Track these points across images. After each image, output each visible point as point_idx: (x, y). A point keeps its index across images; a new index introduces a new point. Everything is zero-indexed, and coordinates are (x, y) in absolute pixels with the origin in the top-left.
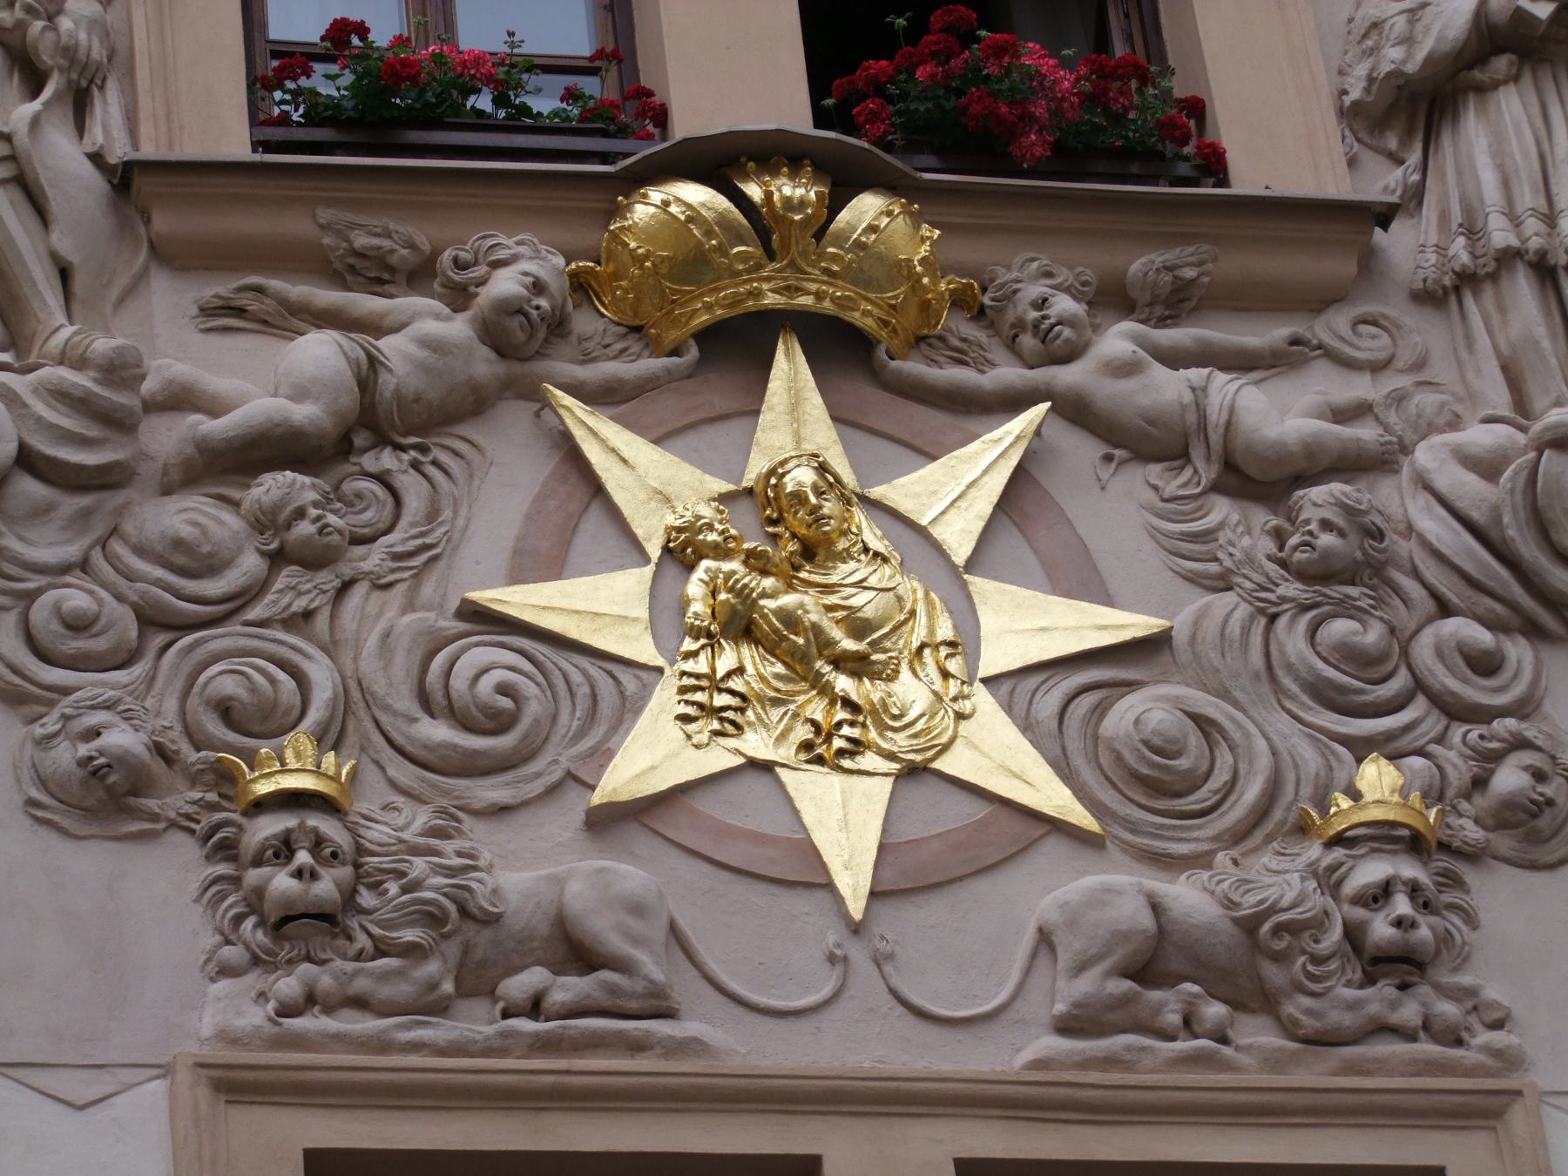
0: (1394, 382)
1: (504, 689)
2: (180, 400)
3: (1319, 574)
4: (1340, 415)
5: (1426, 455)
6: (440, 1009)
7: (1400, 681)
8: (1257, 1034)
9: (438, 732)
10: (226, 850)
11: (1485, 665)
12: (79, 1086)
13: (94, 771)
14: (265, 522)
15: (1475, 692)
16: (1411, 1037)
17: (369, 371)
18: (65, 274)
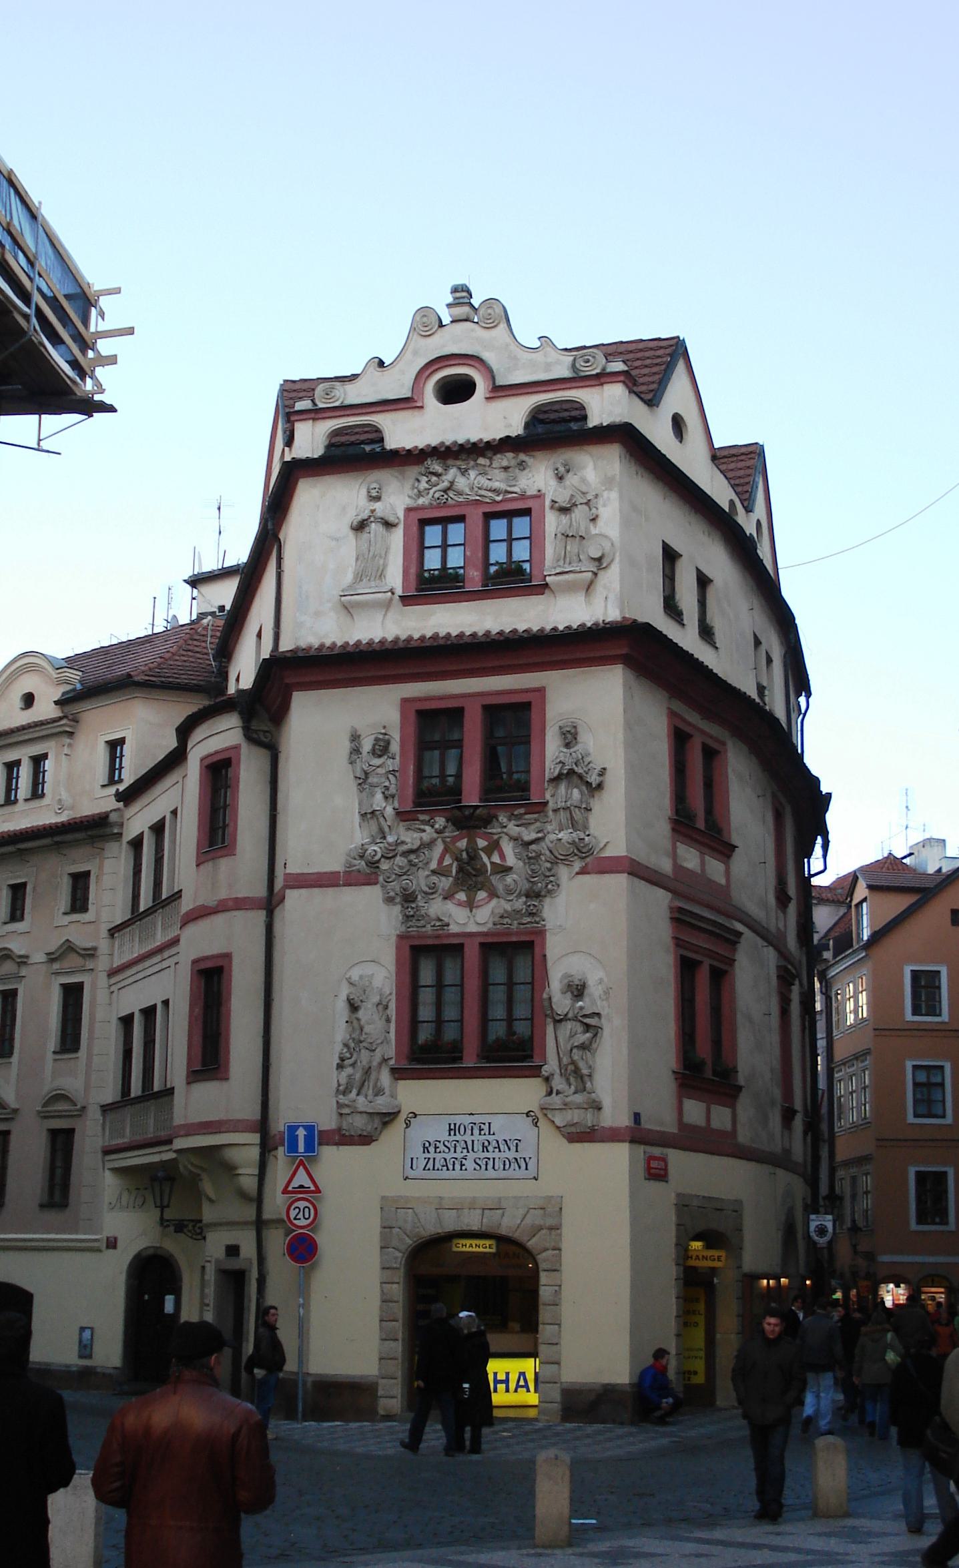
1: (434, 883)
2: (403, 842)
3: (530, 858)
5: (547, 840)
6: (424, 926)
7: (540, 872)
9: (426, 889)
10: (403, 907)
11: (550, 870)
14: (410, 861)
15: (548, 874)
16: (532, 923)
17: (421, 839)
18: (389, 826)
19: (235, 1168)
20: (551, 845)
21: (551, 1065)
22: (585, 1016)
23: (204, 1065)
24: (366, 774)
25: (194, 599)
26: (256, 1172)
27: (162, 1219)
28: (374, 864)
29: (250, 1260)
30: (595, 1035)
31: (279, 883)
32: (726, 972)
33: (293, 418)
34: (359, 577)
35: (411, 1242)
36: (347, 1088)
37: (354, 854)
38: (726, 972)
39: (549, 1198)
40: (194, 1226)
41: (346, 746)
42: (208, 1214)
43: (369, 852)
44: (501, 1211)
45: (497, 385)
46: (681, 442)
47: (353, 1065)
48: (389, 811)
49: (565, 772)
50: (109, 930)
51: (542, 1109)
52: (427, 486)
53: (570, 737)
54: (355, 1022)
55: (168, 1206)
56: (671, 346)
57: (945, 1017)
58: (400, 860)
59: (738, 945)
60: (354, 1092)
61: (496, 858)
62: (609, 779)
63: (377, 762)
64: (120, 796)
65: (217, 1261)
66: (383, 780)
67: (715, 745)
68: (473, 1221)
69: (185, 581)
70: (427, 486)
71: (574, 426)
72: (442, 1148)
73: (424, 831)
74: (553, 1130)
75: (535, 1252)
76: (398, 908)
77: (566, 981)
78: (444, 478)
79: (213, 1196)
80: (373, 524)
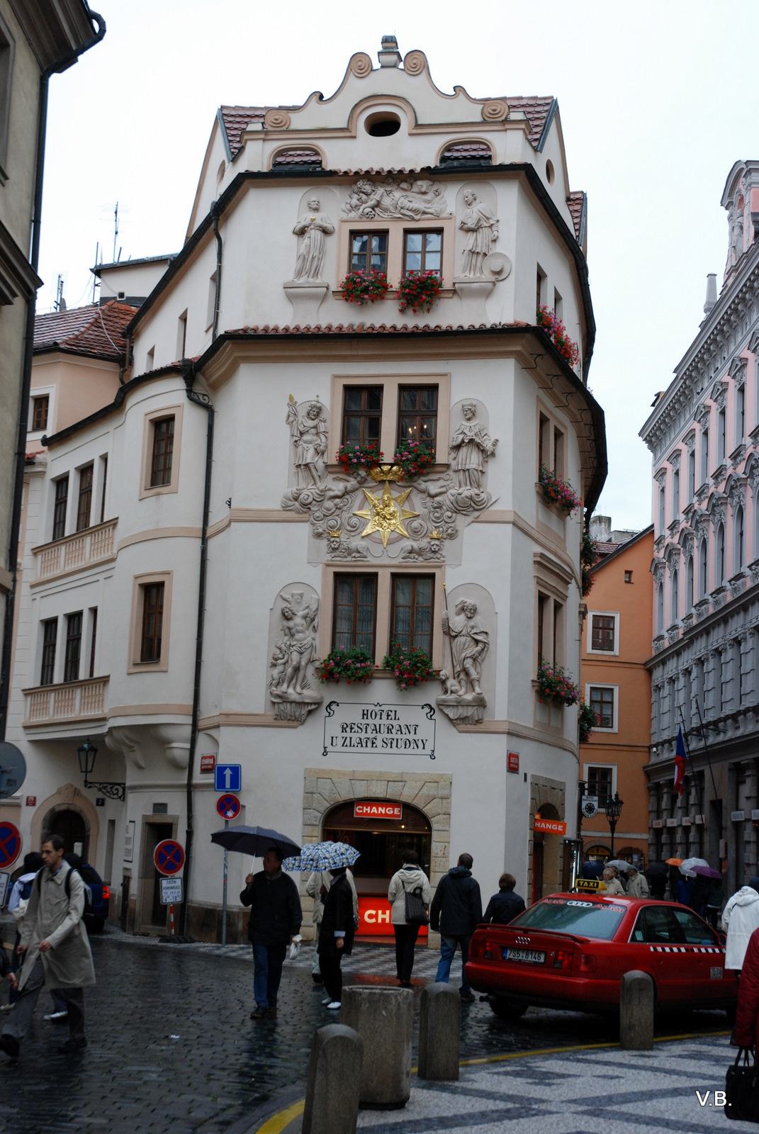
0: (449, 482)
2: (329, 490)
3: (435, 508)
4: (442, 487)
5: (448, 493)
8: (421, 559)
9: (349, 528)
11: (450, 518)
12: (315, 565)
13: (318, 533)
14: (335, 505)
19: (170, 742)
20: (452, 498)
21: (446, 671)
22: (475, 633)
23: (142, 660)
24: (302, 434)
25: (97, 285)
26: (188, 746)
27: (86, 782)
28: (306, 506)
29: (177, 818)
30: (483, 650)
31: (219, 514)
32: (562, 605)
33: (246, 137)
34: (299, 273)
35: (329, 805)
36: (278, 684)
37: (290, 495)
38: (562, 605)
39: (441, 776)
40: (111, 788)
41: (286, 410)
42: (131, 778)
43: (301, 496)
44: (403, 783)
45: (419, 122)
46: (549, 181)
47: (284, 664)
48: (320, 465)
49: (466, 441)
50: (33, 550)
51: (438, 705)
52: (358, 203)
53: (470, 413)
54: (287, 631)
55: (91, 772)
56: (548, 104)
57: (616, 651)
58: (329, 504)
59: (570, 585)
60: (285, 685)
61: (407, 507)
62: (499, 451)
63: (311, 423)
64: (46, 442)
65: (144, 817)
66: (315, 438)
67: (562, 430)
68: (378, 791)
69: (91, 270)
70: (358, 203)
71: (483, 162)
72: (356, 728)
73: (348, 481)
74: (446, 721)
75: (429, 815)
76: (324, 543)
77: (460, 606)
78: (372, 196)
79: (142, 763)
80: (313, 231)
